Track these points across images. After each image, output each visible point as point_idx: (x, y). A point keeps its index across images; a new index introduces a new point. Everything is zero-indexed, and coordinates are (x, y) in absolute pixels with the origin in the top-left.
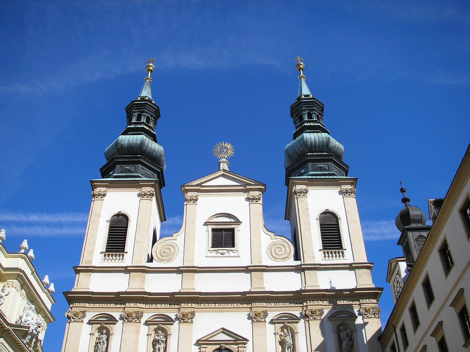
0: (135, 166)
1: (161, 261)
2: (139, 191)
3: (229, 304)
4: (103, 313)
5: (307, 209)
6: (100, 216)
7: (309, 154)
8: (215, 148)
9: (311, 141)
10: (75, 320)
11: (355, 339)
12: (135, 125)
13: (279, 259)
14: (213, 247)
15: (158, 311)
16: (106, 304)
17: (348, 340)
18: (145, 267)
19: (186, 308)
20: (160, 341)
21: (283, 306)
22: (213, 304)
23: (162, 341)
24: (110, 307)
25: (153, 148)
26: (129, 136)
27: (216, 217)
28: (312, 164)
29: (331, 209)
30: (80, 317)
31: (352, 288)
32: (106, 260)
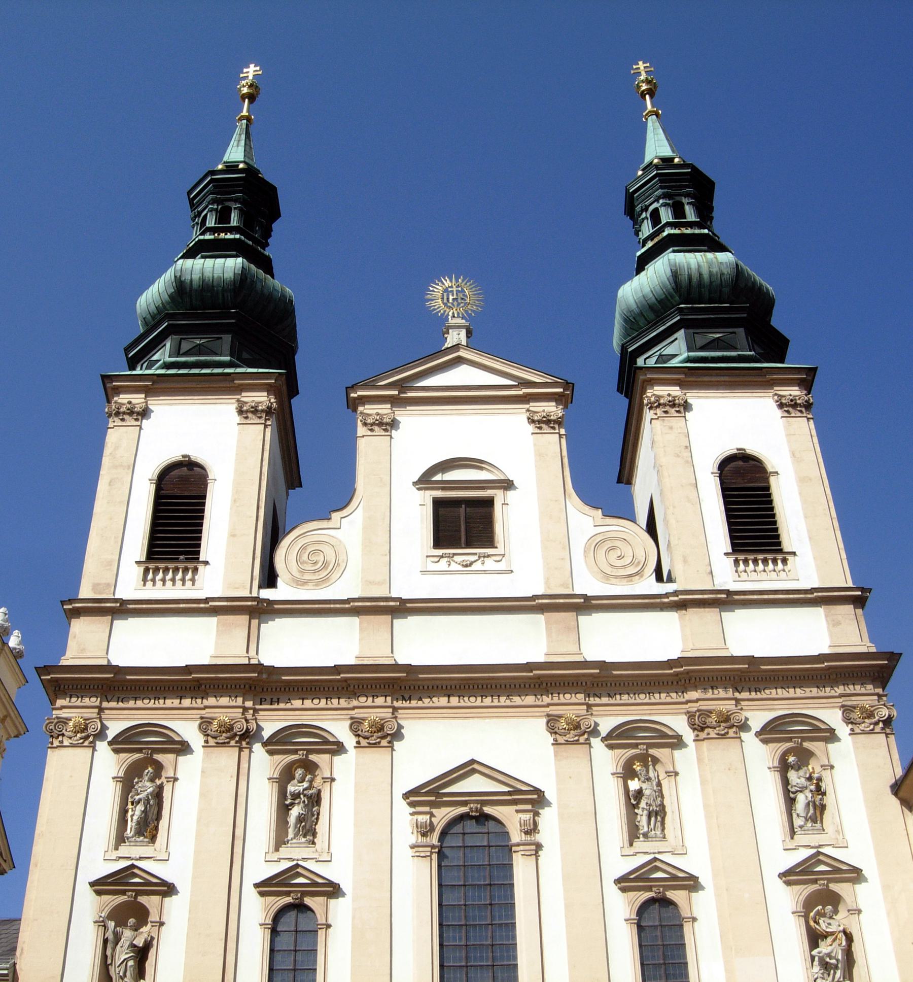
0: (221, 338)
1: (300, 585)
2: (234, 401)
3: (486, 697)
4: (147, 722)
5: (688, 448)
8: (433, 291)
9: (688, 272)
10: (70, 741)
11: (830, 791)
12: (216, 235)
13: (616, 577)
16: (152, 701)
17: (811, 791)
20: (302, 796)
21: (632, 701)
22: (444, 696)
23: (310, 797)
24: (164, 706)
26: (203, 260)
28: (694, 333)
29: (753, 448)
30: (83, 735)
31: (817, 654)
32: (149, 584)
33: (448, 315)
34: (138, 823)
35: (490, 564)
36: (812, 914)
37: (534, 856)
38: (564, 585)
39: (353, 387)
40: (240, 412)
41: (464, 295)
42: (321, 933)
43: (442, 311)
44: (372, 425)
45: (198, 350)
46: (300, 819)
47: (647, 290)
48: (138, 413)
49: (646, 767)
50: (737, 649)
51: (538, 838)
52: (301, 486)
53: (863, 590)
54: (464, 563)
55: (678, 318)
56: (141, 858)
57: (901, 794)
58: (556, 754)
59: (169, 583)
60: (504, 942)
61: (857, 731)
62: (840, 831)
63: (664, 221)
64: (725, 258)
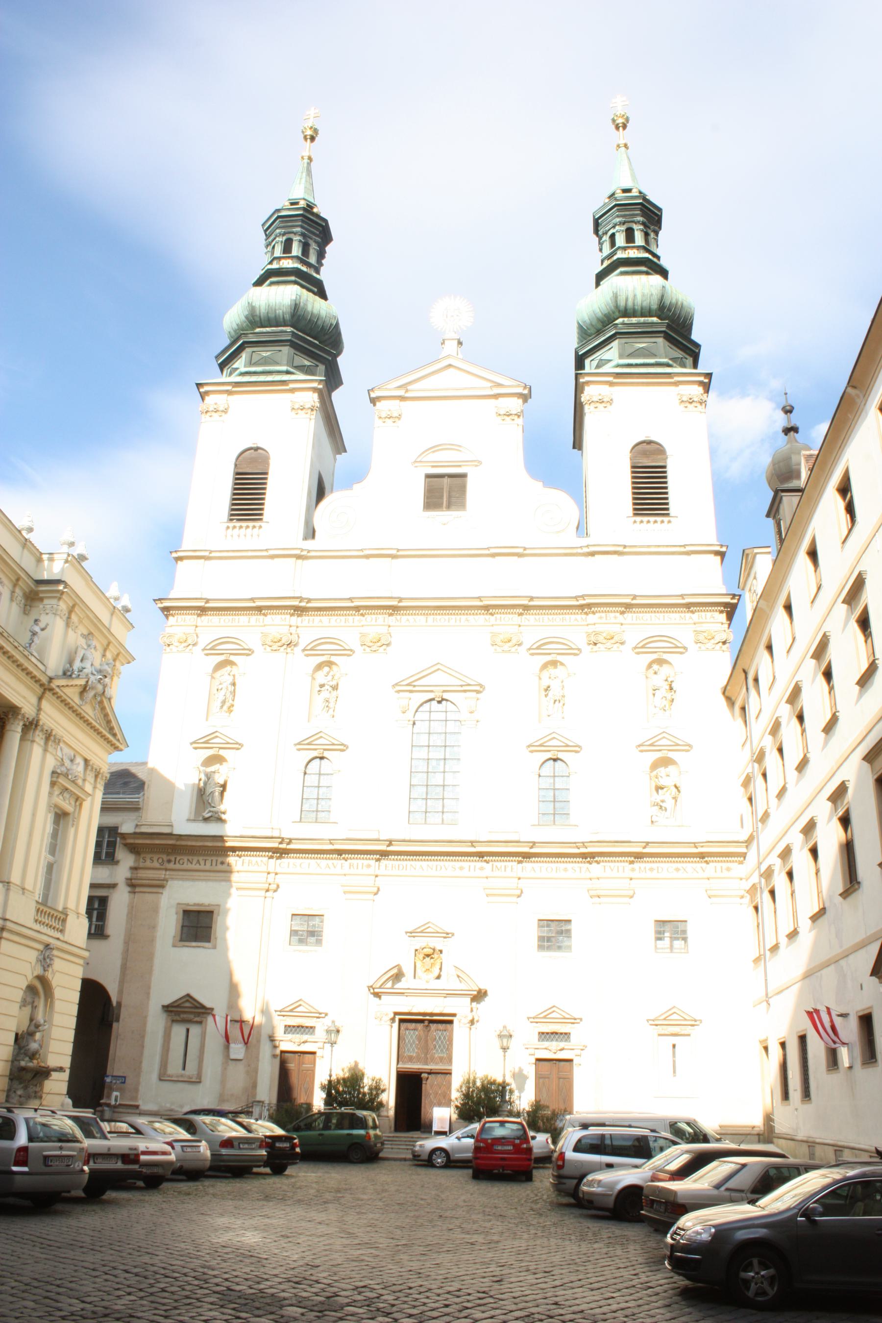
7: (620, 320)
19: (375, 624)
25: (315, 312)
27: (434, 452)
45: (265, 361)
48: (222, 411)
52: (345, 451)
57: (727, 693)
63: (617, 246)
64: (657, 279)
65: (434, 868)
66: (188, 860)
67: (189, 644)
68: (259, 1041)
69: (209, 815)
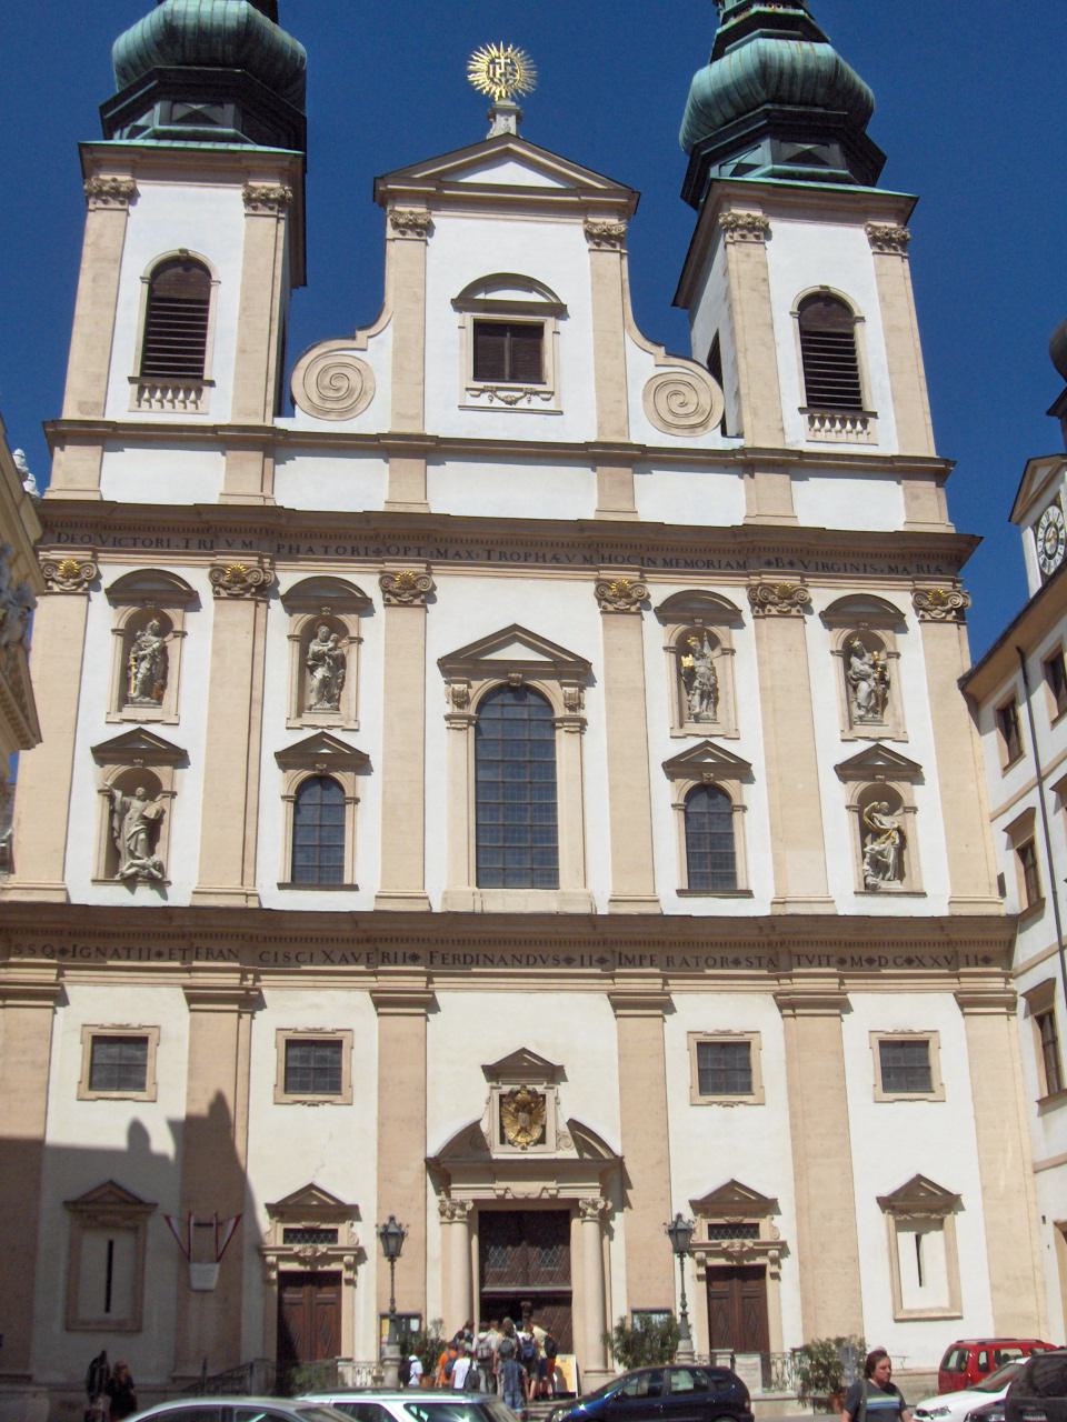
5: (765, 280)
6: (119, 261)
8: (477, 61)
10: (61, 587)
13: (677, 427)
14: (479, 374)
15: (319, 568)
17: (875, 679)
18: (273, 430)
23: (335, 659)
29: (839, 286)
30: (77, 580)
32: (145, 405)
33: (495, 93)
34: (144, 682)
35: (537, 403)
36: (866, 809)
37: (578, 734)
38: (620, 432)
39: (382, 178)
40: (249, 200)
41: (513, 69)
42: (349, 808)
43: (487, 89)
44: (406, 225)
46: (325, 683)
47: (728, 80)
49: (702, 642)
50: (806, 520)
51: (582, 713)
53: (947, 462)
54: (509, 399)
55: (765, 122)
56: (149, 722)
58: (605, 624)
59: (168, 406)
60: (544, 823)
61: (928, 617)
62: (899, 725)
65: (524, 961)
66: (98, 949)
67: (83, 583)
68: (240, 1258)
69: (133, 870)
